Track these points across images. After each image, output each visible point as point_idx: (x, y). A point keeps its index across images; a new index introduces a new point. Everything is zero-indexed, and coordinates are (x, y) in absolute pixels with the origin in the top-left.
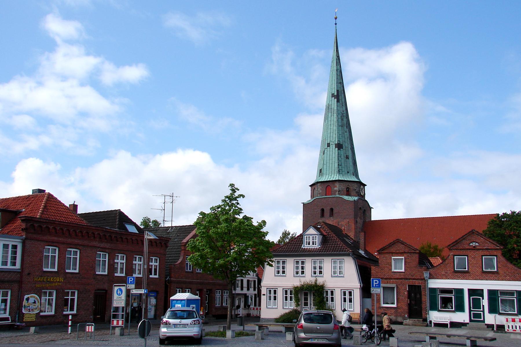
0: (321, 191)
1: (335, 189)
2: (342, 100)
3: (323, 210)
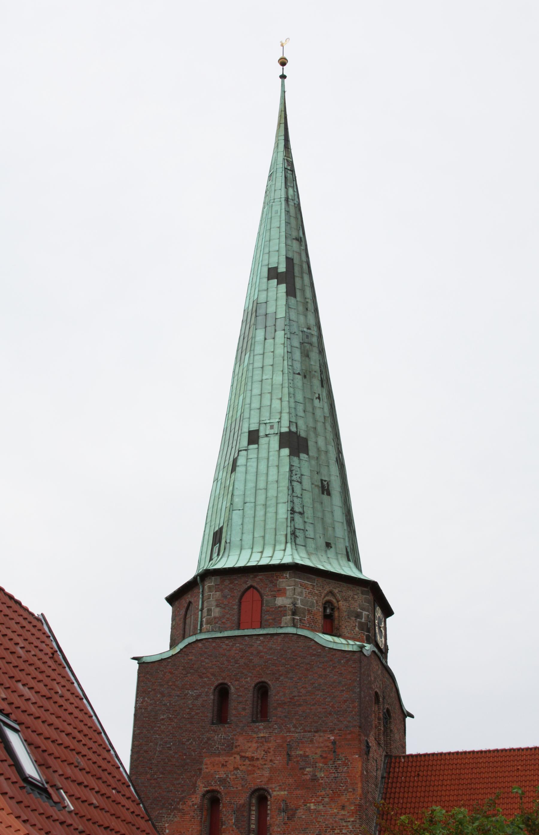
0: (216, 612)
1: (280, 601)
2: (303, 291)
3: (223, 692)
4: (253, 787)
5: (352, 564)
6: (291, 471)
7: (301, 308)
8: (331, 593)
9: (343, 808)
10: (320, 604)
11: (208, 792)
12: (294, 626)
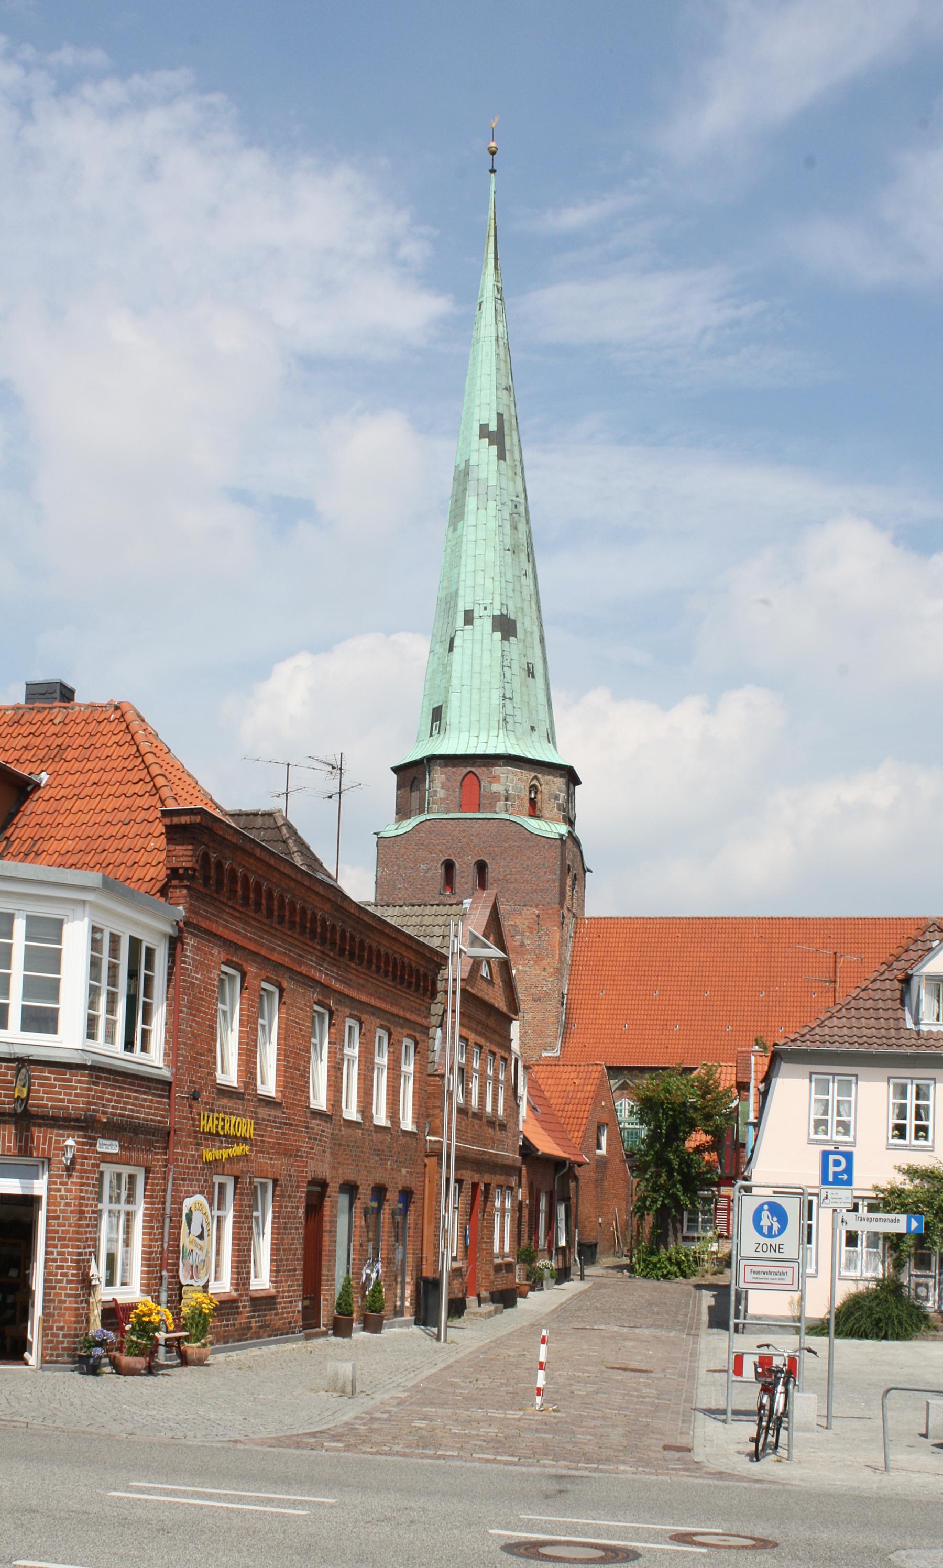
6: (503, 656)
8: (536, 777)
10: (527, 789)
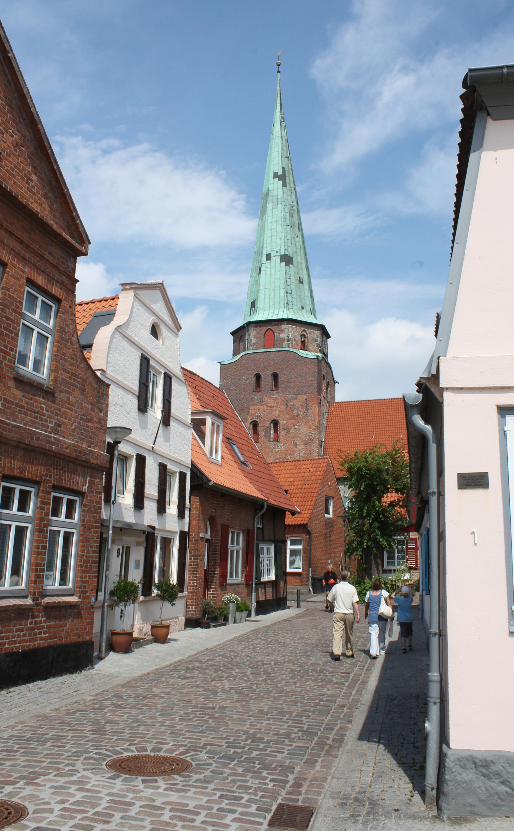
0: (254, 341)
1: (282, 335)
2: (290, 184)
3: (258, 377)
4: (272, 419)
5: (313, 316)
6: (286, 273)
7: (289, 193)
8: (304, 330)
9: (310, 427)
10: (300, 336)
11: (252, 421)
12: (288, 347)
